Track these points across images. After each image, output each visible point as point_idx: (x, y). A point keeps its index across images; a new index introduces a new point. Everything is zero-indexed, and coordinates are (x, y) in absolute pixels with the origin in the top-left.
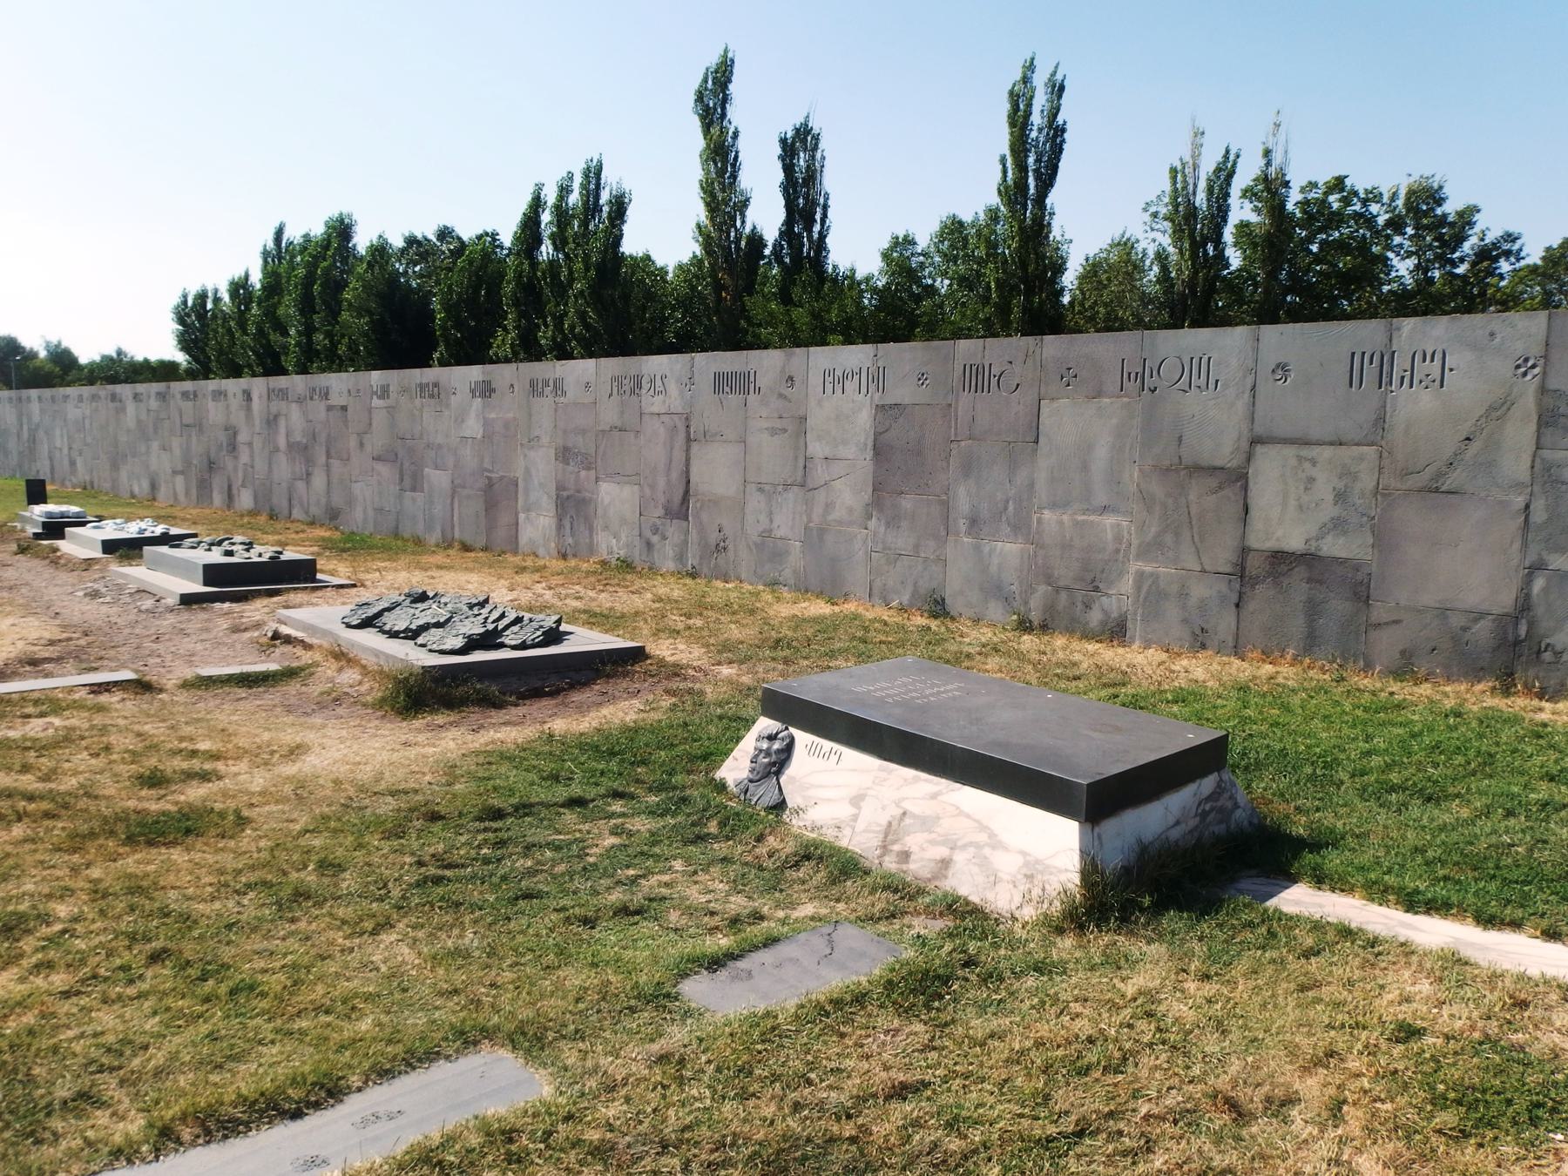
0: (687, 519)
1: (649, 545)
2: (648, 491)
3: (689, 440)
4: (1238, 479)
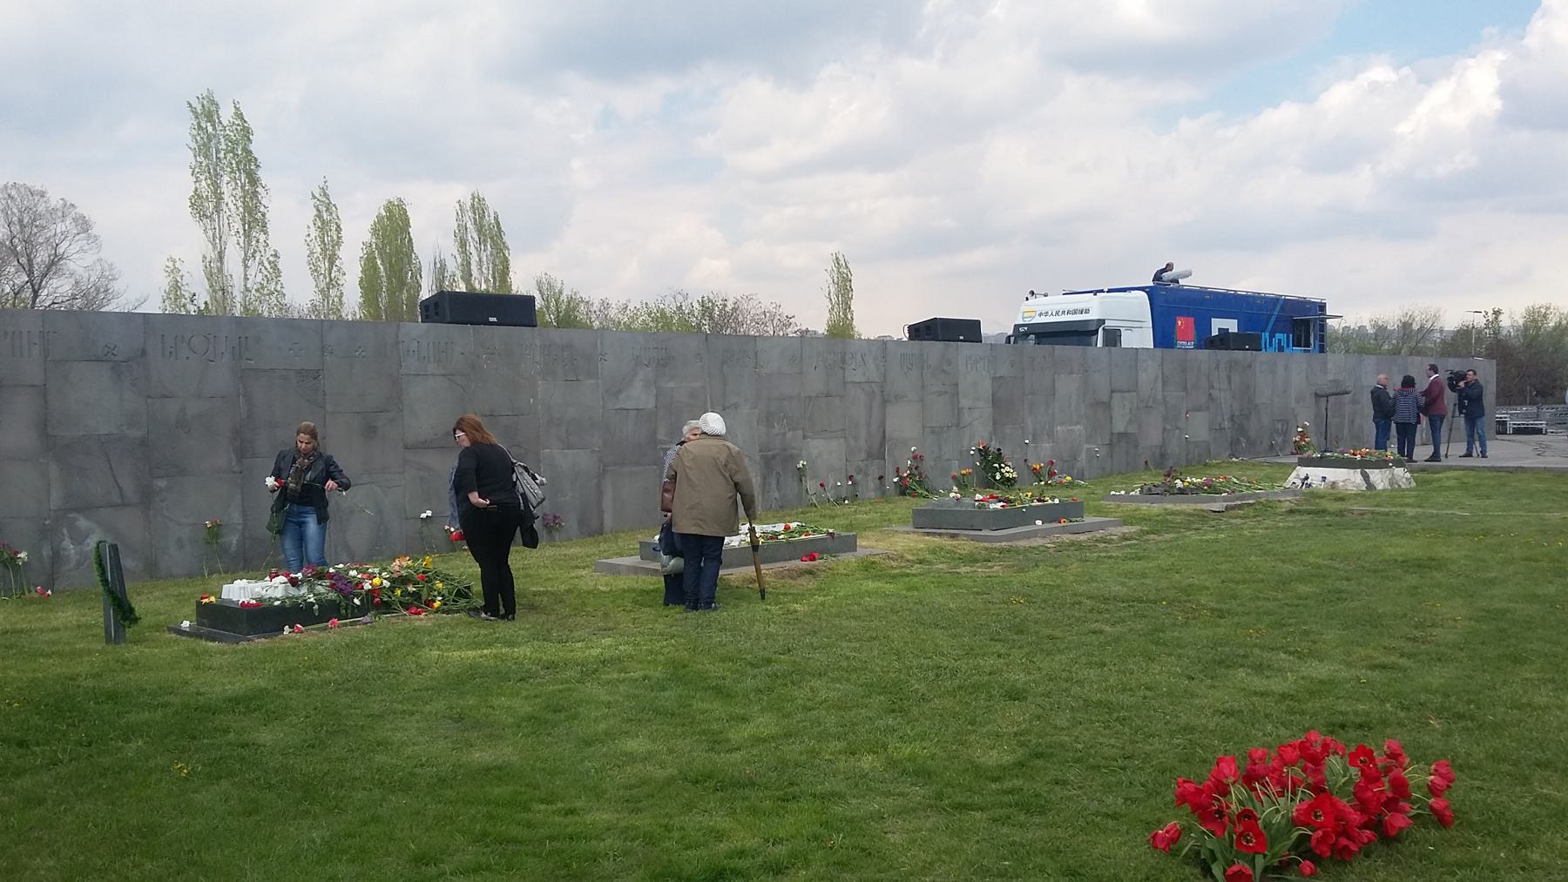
2: (852, 442)
3: (885, 402)
4: (1108, 406)
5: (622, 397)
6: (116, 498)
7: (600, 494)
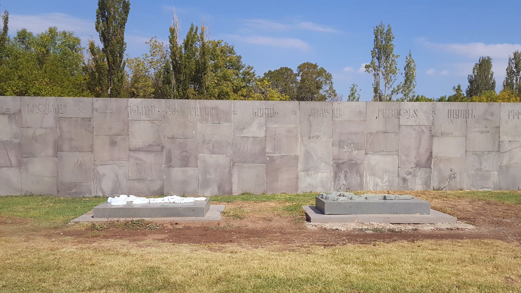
0: (430, 167)
1: (404, 180)
2: (404, 158)
3: (432, 136)
5: (245, 131)
7: (230, 174)
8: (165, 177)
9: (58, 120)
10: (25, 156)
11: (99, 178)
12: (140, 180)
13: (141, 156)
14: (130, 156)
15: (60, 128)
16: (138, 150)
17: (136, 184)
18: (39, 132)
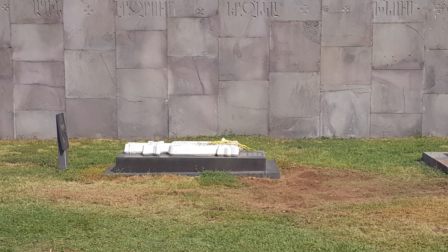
6: (200, 90)
8: (424, 109)
9: (272, 25)
10: (224, 78)
11: (326, 110)
12: (385, 113)
13: (390, 77)
14: (372, 78)
15: (274, 37)
16: (385, 68)
17: (381, 118)
18: (244, 43)
